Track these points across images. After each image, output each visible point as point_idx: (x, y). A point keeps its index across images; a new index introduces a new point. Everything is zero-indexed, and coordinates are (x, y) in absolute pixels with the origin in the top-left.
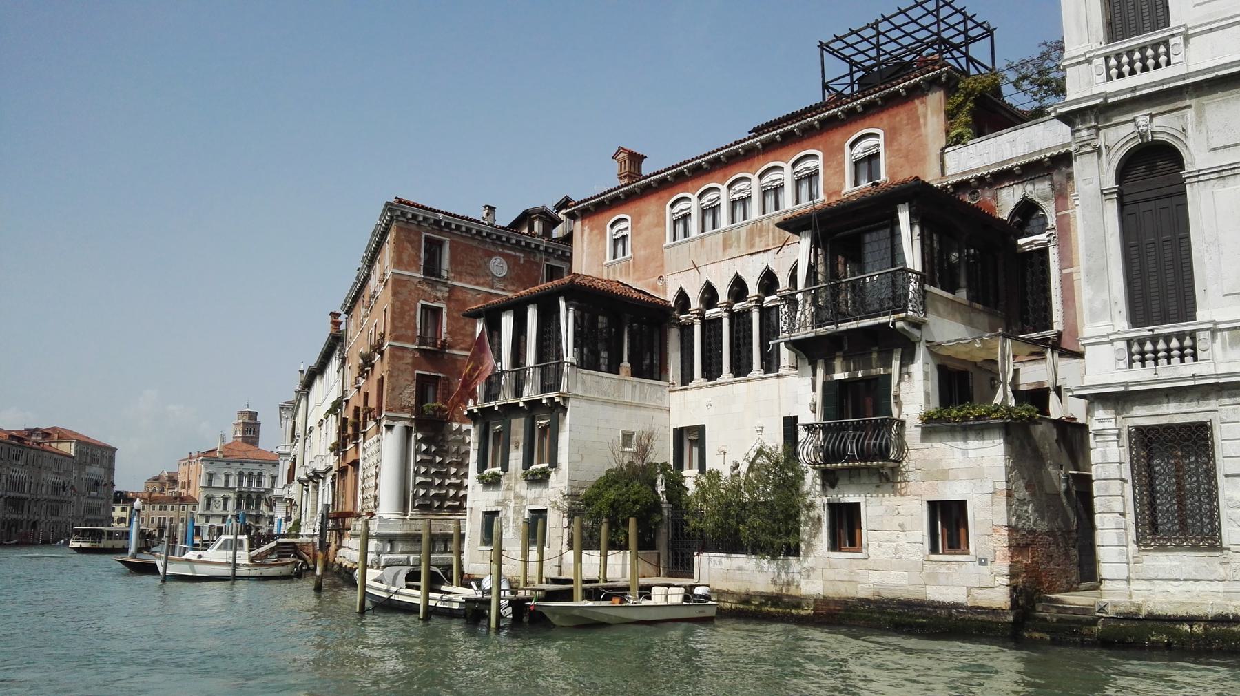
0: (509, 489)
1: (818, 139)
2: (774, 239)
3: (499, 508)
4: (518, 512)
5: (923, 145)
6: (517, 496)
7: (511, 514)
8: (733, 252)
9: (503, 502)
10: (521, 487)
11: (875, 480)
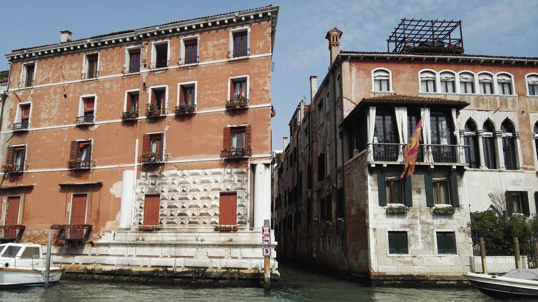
0: (414, 217)
1: (511, 69)
2: (491, 106)
3: (407, 230)
4: (426, 233)
6: (422, 223)
7: (419, 234)
9: (409, 226)
10: (428, 218)
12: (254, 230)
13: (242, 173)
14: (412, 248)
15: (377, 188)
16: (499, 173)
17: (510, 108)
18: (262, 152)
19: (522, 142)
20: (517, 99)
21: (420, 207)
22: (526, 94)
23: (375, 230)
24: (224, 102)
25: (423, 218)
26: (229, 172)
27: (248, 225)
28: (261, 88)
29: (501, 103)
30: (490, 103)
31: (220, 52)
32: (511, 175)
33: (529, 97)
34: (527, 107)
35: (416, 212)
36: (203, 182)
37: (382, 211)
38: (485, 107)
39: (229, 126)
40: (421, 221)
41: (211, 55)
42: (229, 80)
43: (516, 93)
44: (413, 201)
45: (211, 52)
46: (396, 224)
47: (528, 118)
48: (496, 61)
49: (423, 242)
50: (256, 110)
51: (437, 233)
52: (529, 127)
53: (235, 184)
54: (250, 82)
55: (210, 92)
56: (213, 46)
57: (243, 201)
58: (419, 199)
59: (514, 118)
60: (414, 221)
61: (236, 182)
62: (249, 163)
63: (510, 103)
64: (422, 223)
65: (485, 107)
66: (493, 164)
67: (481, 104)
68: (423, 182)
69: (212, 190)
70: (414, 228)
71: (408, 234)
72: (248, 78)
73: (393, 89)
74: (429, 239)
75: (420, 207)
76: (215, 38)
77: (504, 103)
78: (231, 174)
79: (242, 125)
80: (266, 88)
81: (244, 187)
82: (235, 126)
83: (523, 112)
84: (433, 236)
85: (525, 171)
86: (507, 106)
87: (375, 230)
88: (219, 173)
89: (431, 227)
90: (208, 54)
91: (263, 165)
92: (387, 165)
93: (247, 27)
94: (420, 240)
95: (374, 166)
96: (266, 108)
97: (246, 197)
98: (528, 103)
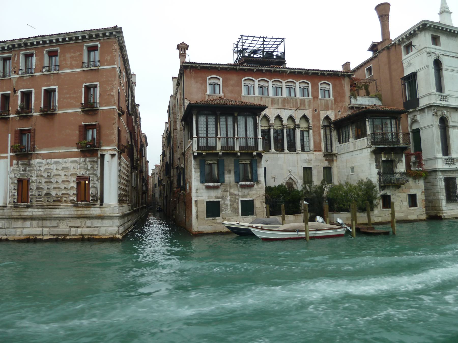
0: (225, 191)
2: (293, 106)
3: (220, 200)
5: (344, 93)
6: (231, 194)
7: (228, 202)
8: (276, 106)
9: (222, 197)
11: (394, 189)
12: (104, 205)
13: (94, 161)
14: (223, 213)
15: (199, 170)
16: (296, 154)
17: (307, 107)
18: (108, 145)
19: (314, 132)
20: (312, 101)
21: (230, 183)
22: (318, 96)
23: (196, 201)
24: (79, 104)
25: (232, 191)
26: (84, 160)
27: (99, 202)
28: (108, 94)
29: (300, 104)
30: (293, 104)
31: (76, 63)
32: (305, 156)
33: (321, 100)
34: (319, 106)
35: (227, 187)
36: (63, 169)
37: (202, 186)
38: (289, 106)
39: (83, 124)
40: (231, 194)
41: (69, 65)
42: (83, 86)
43: (312, 96)
44: (225, 179)
45: (69, 63)
46: (212, 196)
47: (319, 114)
48: (298, 72)
49: (231, 208)
50: (105, 111)
51: (241, 201)
52: (319, 120)
53: (88, 170)
54: (100, 88)
55: (68, 96)
56: (70, 58)
57: (95, 184)
58: (229, 178)
59: (309, 114)
60: (225, 193)
61: (89, 168)
62: (99, 153)
63: (306, 104)
64: (231, 194)
65: (289, 106)
66: (292, 147)
67: (286, 104)
68: (233, 165)
69: (71, 175)
70: (225, 198)
71: (221, 203)
72: (98, 85)
73: (223, 92)
74: (235, 206)
75: (230, 183)
76: (72, 51)
77: (303, 103)
78: (85, 161)
79: (94, 123)
80: (112, 94)
81: (95, 172)
82: (88, 124)
83: (316, 110)
84: (238, 203)
85: (315, 153)
86: (304, 106)
87: (196, 201)
88: (76, 162)
89: (237, 197)
90: (67, 64)
91: (110, 156)
92: (206, 153)
93: (98, 43)
94: (229, 207)
95: (196, 154)
96: (112, 110)
97: (97, 180)
98: (319, 103)
